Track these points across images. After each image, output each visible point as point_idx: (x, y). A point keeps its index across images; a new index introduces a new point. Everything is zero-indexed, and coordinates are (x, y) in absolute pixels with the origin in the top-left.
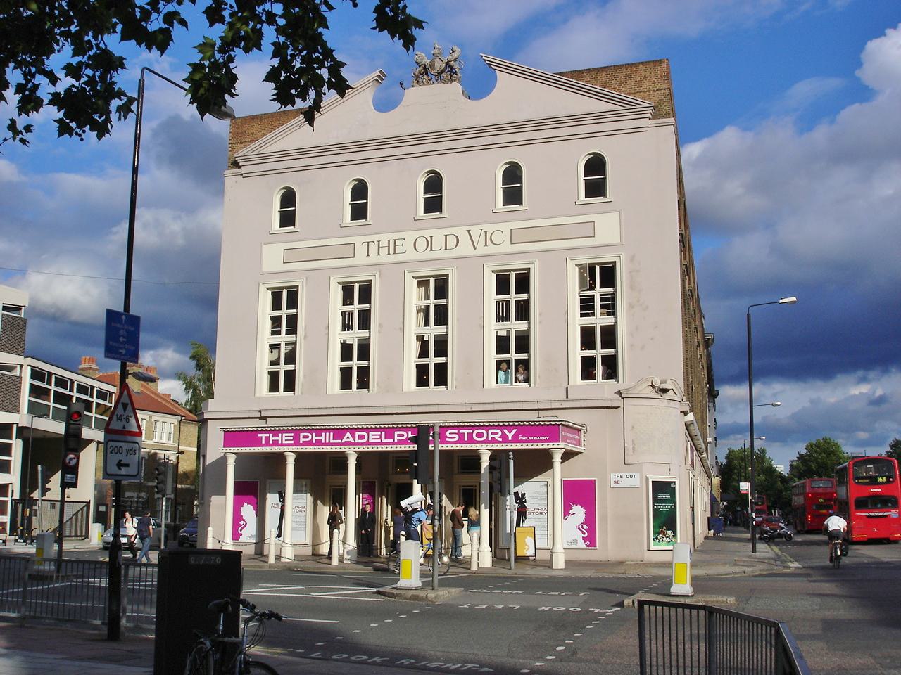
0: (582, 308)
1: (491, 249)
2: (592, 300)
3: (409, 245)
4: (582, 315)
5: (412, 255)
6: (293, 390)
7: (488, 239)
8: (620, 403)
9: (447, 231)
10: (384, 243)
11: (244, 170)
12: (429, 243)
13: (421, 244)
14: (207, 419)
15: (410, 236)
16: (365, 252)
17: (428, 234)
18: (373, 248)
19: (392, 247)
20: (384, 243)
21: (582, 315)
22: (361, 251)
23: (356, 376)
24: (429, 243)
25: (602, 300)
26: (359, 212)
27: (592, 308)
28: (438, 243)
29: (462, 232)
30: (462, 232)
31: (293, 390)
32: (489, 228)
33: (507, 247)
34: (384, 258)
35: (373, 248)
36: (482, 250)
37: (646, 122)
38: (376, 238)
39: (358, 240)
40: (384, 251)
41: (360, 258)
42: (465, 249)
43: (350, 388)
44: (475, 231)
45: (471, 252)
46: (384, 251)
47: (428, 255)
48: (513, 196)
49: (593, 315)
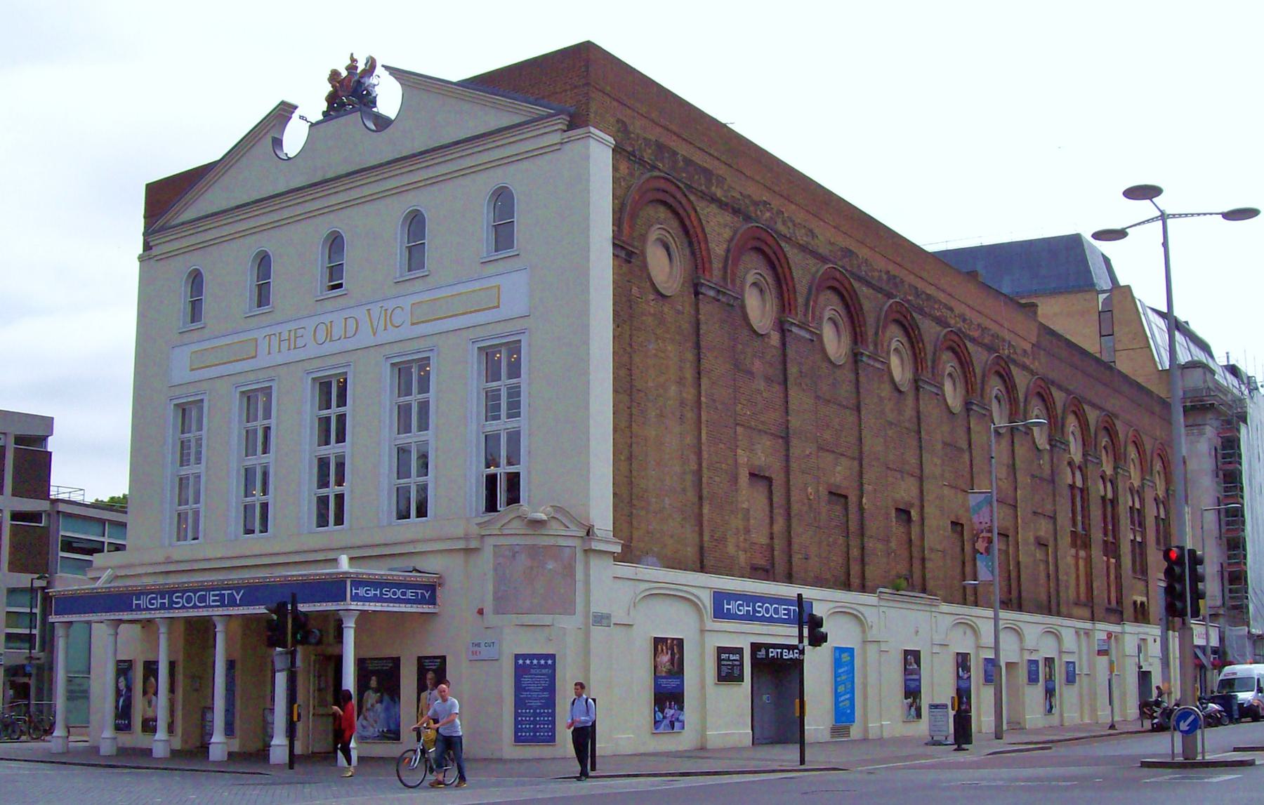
5: (313, 350)
8: (474, 544)
9: (346, 314)
11: (155, 252)
13: (321, 336)
15: (311, 324)
17: (327, 319)
22: (263, 346)
23: (330, 511)
24: (329, 334)
27: (498, 407)
28: (337, 331)
29: (361, 313)
32: (390, 305)
33: (406, 332)
36: (383, 337)
37: (556, 138)
39: (259, 335)
42: (365, 337)
45: (371, 341)
46: (285, 345)
47: (329, 348)
48: (415, 255)
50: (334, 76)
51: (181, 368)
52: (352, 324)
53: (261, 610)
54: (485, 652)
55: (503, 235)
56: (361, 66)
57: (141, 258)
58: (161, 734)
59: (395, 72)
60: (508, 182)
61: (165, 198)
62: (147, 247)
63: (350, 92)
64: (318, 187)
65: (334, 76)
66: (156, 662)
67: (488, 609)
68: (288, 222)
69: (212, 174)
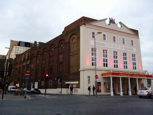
1: (122, 49)
6: (107, 67)
10: (109, 45)
12: (115, 46)
13: (114, 46)
14: (80, 71)
15: (113, 45)
20: (109, 45)
22: (106, 45)
28: (116, 47)
30: (119, 46)
31: (107, 67)
34: (109, 47)
36: (121, 49)
40: (109, 46)
41: (106, 46)
42: (119, 48)
46: (109, 46)
50: (110, 19)
56: (113, 19)
59: (120, 23)
65: (110, 19)
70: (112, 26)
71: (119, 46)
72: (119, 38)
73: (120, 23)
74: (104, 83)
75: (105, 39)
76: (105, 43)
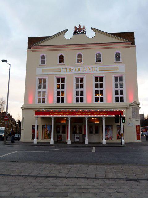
0: (115, 86)
2: (118, 84)
3: (74, 70)
4: (115, 87)
5: (75, 72)
7: (93, 69)
8: (129, 107)
11: (32, 50)
12: (79, 69)
13: (77, 70)
15: (74, 68)
16: (64, 71)
18: (65, 70)
19: (70, 70)
20: (68, 69)
21: (115, 87)
22: (62, 70)
24: (79, 69)
25: (120, 84)
26: (61, 61)
28: (81, 69)
30: (87, 68)
35: (65, 70)
37: (130, 46)
38: (66, 68)
40: (68, 71)
42: (88, 71)
43: (59, 102)
44: (90, 68)
45: (90, 72)
46: (68, 71)
49: (118, 87)
50: (76, 27)
51: (40, 71)
52: (85, 69)
53: (114, 116)
54: (131, 125)
55: (118, 59)
56: (82, 27)
57: (27, 51)
58: (35, 139)
60: (118, 51)
61: (33, 42)
62: (29, 48)
63: (79, 31)
64: (70, 46)
65: (76, 27)
66: (35, 125)
67: (131, 118)
68: (69, 50)
69: (49, 38)
70: (80, 39)
71: (86, 67)
72: (89, 55)
73: (92, 29)
74: (43, 126)
75: (61, 61)
76: (61, 68)
